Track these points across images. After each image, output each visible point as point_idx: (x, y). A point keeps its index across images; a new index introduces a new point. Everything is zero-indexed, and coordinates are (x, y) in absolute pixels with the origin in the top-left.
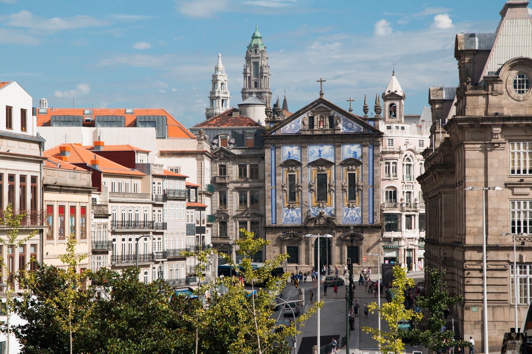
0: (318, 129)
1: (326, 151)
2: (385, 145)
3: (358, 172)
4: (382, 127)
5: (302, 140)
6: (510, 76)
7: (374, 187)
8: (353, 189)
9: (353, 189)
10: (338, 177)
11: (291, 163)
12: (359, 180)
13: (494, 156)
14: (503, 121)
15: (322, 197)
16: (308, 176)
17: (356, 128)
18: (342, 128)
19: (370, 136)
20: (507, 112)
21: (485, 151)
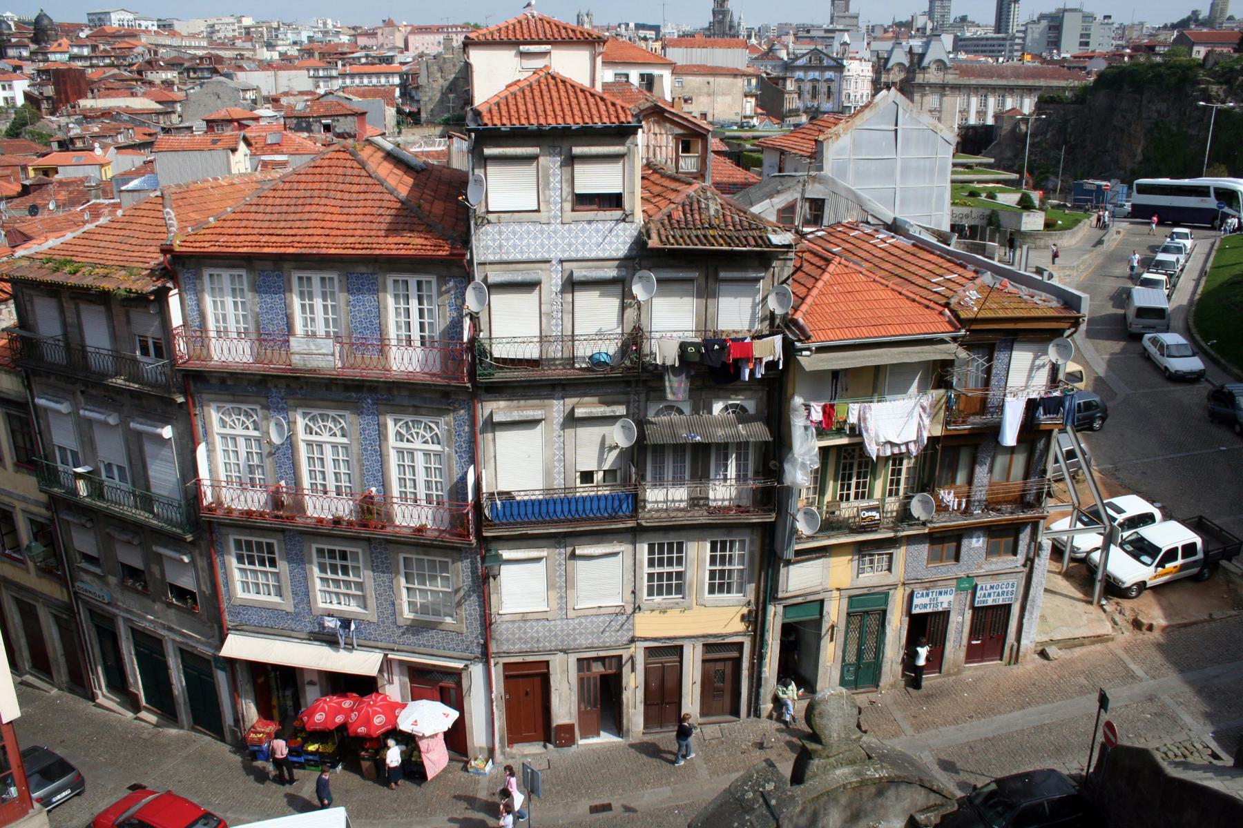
0: (814, 63)
1: (816, 74)
2: (846, 73)
3: (833, 85)
4: (845, 62)
5: (806, 68)
6: (933, 67)
7: (840, 93)
8: (829, 94)
9: (829, 94)
10: (823, 88)
11: (799, 80)
12: (832, 89)
13: (926, 99)
14: (931, 86)
15: (814, 96)
16: (807, 87)
17: (832, 63)
18: (825, 63)
19: (839, 68)
20: (932, 81)
21: (922, 97)
